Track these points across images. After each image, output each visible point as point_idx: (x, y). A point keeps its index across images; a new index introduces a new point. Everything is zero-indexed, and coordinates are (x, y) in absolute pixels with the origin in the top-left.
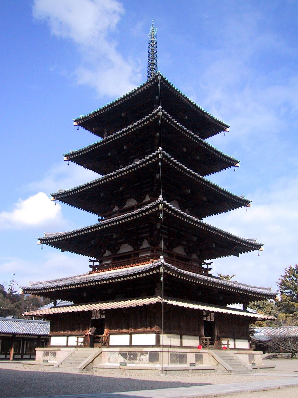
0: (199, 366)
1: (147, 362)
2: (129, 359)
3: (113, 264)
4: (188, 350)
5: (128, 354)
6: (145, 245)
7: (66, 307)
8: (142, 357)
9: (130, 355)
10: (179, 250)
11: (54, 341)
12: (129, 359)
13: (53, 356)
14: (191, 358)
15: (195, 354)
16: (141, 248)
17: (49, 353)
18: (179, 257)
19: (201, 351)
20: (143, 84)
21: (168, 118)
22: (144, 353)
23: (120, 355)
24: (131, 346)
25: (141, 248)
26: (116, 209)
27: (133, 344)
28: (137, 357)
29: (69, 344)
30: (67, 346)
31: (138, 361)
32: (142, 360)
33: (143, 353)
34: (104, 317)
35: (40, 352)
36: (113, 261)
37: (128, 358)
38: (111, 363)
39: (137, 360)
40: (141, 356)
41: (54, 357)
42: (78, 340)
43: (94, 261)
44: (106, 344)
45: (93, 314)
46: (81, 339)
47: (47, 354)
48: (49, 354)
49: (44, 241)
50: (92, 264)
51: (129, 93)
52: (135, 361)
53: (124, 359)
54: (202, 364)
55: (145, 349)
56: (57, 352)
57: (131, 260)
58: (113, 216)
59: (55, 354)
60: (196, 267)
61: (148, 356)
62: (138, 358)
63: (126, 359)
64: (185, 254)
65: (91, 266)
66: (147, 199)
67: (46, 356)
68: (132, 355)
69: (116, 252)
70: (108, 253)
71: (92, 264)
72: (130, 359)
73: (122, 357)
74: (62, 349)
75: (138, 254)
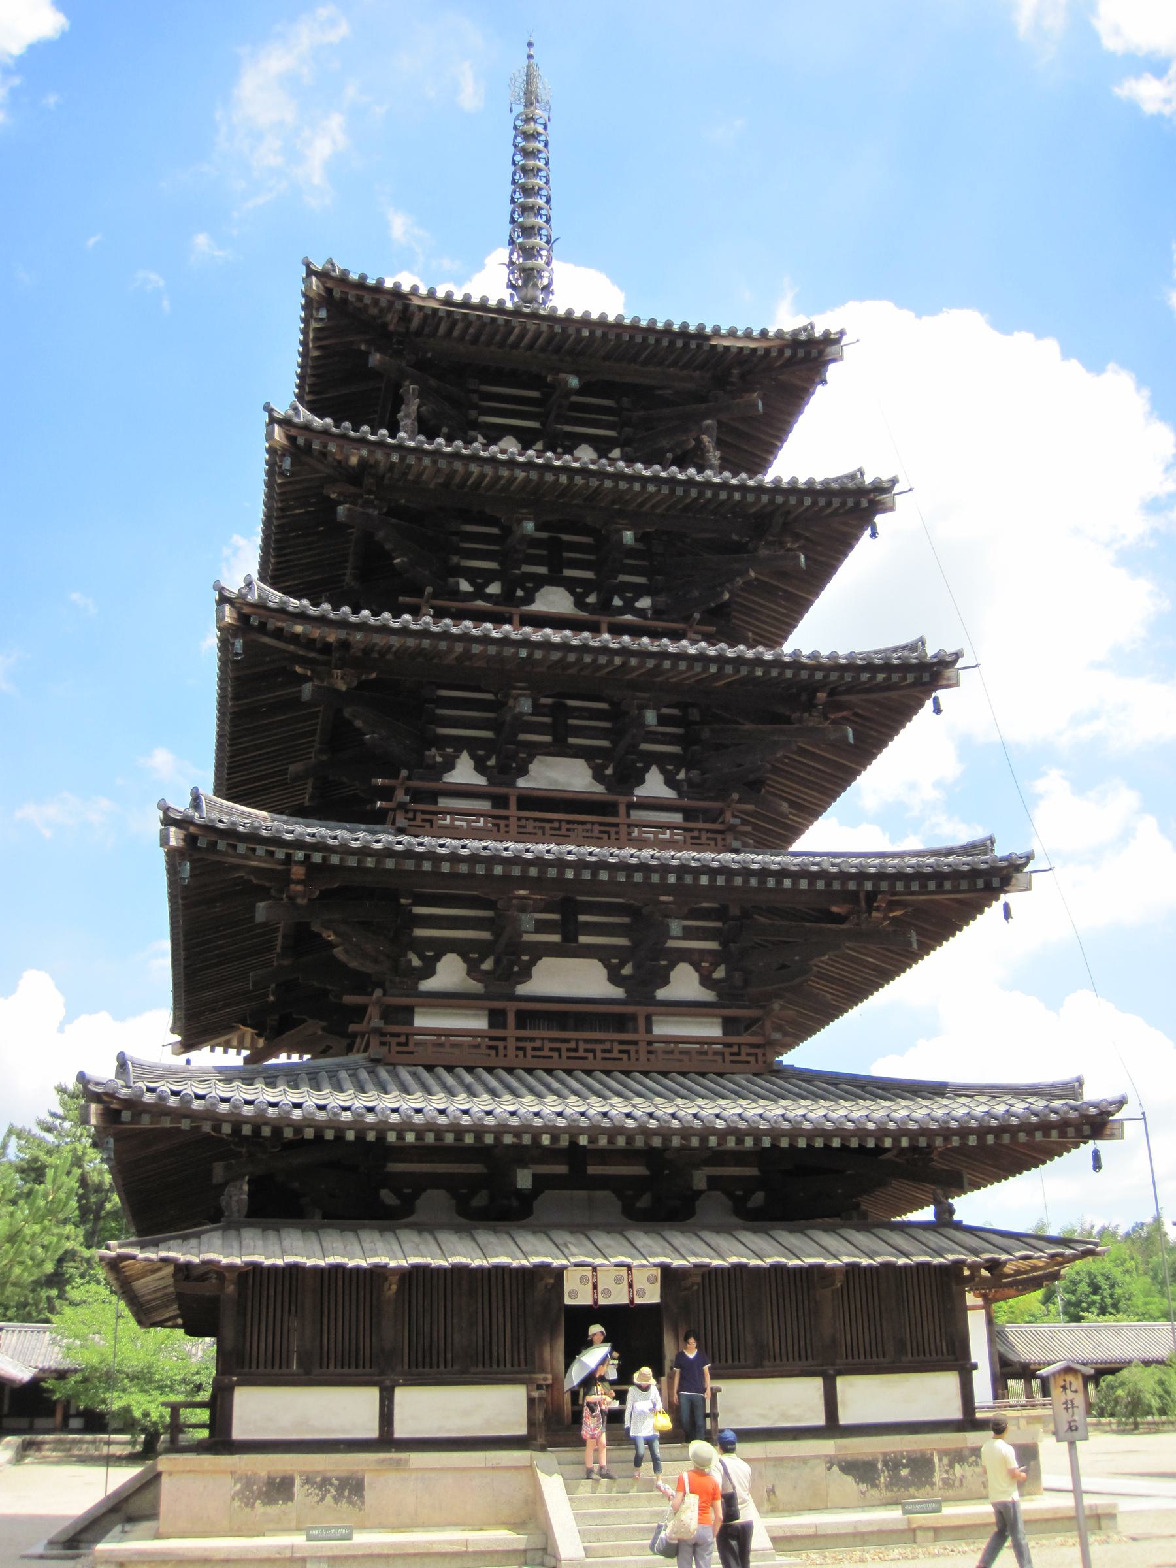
2: (887, 1487)
3: (492, 1038)
5: (880, 1465)
12: (888, 1487)
13: (336, 1499)
17: (298, 1482)
20: (764, 333)
22: (966, 1452)
23: (835, 1468)
26: (464, 773)
27: (845, 1418)
28: (932, 1471)
29: (401, 1431)
31: (938, 1491)
32: (957, 1483)
37: (882, 1480)
38: (781, 1511)
39: (933, 1484)
40: (951, 1465)
41: (344, 1505)
51: (685, 326)
52: (923, 1494)
53: (863, 1487)
57: (635, 1043)
58: (444, 803)
59: (352, 1488)
62: (938, 1477)
63: (874, 1484)
66: (654, 786)
68: (904, 1466)
72: (895, 1485)
73: (849, 1479)
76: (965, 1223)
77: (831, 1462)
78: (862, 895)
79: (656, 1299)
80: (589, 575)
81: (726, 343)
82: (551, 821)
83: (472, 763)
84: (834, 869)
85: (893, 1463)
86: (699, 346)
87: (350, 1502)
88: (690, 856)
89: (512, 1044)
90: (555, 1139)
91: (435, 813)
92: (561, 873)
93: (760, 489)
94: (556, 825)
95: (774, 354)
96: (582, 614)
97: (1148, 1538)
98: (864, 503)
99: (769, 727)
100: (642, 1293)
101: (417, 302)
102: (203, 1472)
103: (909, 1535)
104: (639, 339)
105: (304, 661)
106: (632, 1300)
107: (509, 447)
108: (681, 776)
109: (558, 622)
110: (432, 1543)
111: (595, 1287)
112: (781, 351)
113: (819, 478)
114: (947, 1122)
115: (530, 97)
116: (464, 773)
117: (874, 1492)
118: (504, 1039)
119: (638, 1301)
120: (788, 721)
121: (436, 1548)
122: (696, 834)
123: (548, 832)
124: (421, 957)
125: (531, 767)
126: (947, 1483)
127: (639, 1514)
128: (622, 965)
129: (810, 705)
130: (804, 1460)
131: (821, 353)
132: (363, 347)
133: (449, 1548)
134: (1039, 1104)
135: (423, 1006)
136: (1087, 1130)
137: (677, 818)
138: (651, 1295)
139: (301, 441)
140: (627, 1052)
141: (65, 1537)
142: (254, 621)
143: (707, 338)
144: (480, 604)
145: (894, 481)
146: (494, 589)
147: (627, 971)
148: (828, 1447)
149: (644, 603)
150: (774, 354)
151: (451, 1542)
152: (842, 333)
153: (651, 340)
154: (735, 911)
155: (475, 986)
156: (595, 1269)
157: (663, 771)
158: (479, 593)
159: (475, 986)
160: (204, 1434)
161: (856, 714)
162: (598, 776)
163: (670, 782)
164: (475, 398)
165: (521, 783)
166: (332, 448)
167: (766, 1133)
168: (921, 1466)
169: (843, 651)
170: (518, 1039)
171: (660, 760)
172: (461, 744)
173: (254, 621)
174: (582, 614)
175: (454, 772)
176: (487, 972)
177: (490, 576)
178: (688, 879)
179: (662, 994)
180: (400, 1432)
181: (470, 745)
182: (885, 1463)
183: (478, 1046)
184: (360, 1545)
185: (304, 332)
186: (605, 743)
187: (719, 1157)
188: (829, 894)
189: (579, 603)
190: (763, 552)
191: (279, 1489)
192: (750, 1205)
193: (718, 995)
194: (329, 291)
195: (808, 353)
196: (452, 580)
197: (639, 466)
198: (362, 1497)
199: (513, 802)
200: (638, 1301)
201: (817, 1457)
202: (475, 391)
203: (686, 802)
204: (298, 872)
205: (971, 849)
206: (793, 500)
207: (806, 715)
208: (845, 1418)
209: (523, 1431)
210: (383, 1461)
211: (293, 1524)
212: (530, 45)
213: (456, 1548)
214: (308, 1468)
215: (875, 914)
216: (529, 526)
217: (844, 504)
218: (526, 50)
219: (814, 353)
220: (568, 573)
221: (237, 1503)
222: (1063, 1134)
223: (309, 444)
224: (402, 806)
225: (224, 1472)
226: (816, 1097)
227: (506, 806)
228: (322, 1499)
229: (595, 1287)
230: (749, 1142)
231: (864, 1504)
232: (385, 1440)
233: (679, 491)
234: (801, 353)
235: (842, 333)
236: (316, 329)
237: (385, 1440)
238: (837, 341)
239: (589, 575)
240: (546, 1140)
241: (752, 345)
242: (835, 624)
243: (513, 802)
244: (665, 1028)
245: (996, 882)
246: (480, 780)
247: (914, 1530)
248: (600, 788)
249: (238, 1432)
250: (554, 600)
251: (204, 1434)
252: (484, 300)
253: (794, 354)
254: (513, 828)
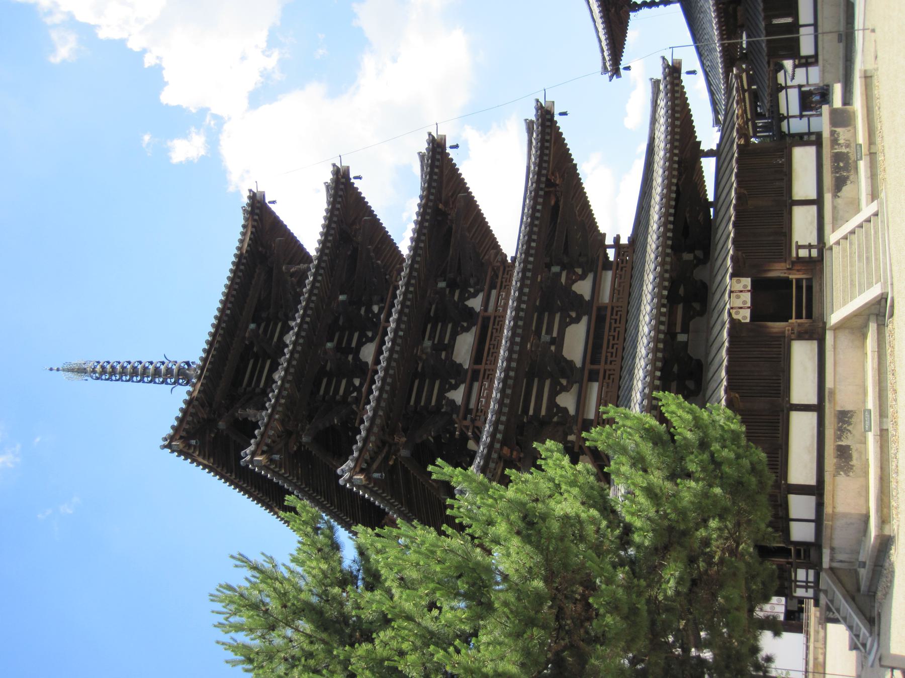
1: (852, 131)
8: (841, 141)
12: (848, 171)
13: (849, 424)
17: (840, 443)
23: (839, 194)
26: (457, 396)
27: (813, 195)
33: (835, 141)
39: (848, 153)
40: (839, 144)
41: (853, 420)
45: (739, 317)
51: (233, 263)
52: (852, 157)
53: (848, 182)
56: (838, 408)
58: (472, 405)
59: (844, 417)
61: (838, 130)
62: (844, 150)
66: (476, 303)
67: (850, 457)
73: (845, 189)
76: (718, 142)
77: (835, 196)
78: (547, 190)
79: (749, 279)
80: (356, 335)
81: (246, 245)
82: (489, 349)
83: (452, 392)
84: (534, 185)
85: (836, 169)
86: (245, 258)
87: (851, 417)
88: (514, 293)
89: (608, 367)
90: (664, 306)
91: (477, 410)
92: (522, 310)
93: (319, 258)
94: (492, 347)
95: (256, 224)
96: (377, 339)
97: (876, 51)
98: (343, 180)
99: (453, 240)
100: (745, 286)
101: (195, 394)
102: (834, 491)
103: (872, 155)
104: (237, 287)
105: (386, 459)
106: (749, 291)
107: (290, 338)
108: (472, 290)
109: (379, 352)
110: (873, 368)
111: (741, 308)
112: (255, 220)
113: (325, 206)
114: (649, 349)
115: (81, 371)
116: (457, 396)
117: (851, 178)
118: (605, 371)
119: (749, 288)
120: (451, 228)
121: (876, 365)
122: (492, 347)
123: (495, 350)
124: (556, 414)
125: (458, 362)
126: (848, 146)
127: (859, 268)
128: (570, 317)
129: (444, 214)
130: (834, 208)
131: (259, 202)
132: (213, 435)
133: (876, 360)
134: (662, 95)
135: (583, 414)
136: (675, 75)
137: (494, 293)
138: (747, 282)
139: (265, 448)
140: (609, 375)
141: (869, 626)
142: (364, 466)
143: (241, 254)
144: (364, 389)
145: (334, 165)
146: (357, 382)
147: (574, 314)
148: (828, 197)
149: (376, 309)
150: (256, 224)
151: (873, 359)
152: (250, 191)
153: (238, 280)
154: (548, 260)
155: (575, 388)
156: (732, 308)
157: (468, 299)
158: (358, 389)
159: (575, 388)
160: (811, 573)
161: (453, 195)
162: (467, 330)
163: (475, 295)
164: (249, 389)
165: (466, 366)
166: (271, 433)
167: (655, 355)
168: (838, 157)
169: (419, 192)
170: (606, 363)
171: (463, 299)
172: (441, 396)
173: (364, 466)
174: (377, 339)
175: (456, 400)
176: (568, 382)
177: (350, 383)
178: (532, 252)
179: (587, 297)
180: (812, 481)
181: (442, 392)
182: (837, 173)
183: (608, 384)
184: (874, 406)
185: (199, 464)
186: (450, 326)
187: (671, 324)
188: (544, 204)
189: (371, 340)
190: (360, 239)
191: (844, 453)
192: (702, 257)
193: (591, 271)
194: (181, 438)
195: (258, 208)
196: (349, 399)
197: (307, 281)
198: (848, 412)
199: (477, 367)
200: (749, 304)
201: (833, 202)
202: (245, 389)
203: (486, 287)
204: (506, 451)
205: (530, 131)
206: (337, 213)
207: (449, 217)
208: (813, 195)
209: (814, 344)
210: (829, 400)
211: (863, 446)
212: (51, 369)
213: (876, 356)
214: (832, 437)
215: (557, 182)
216: (329, 345)
217: (342, 190)
218: (54, 372)
219: (258, 205)
220: (354, 345)
221: (851, 474)
222: (677, 92)
223: (267, 445)
224: (473, 421)
225: (834, 481)
226: (649, 206)
227: (479, 371)
228: (850, 431)
229: (741, 308)
230: (663, 319)
231: (857, 182)
232: (819, 408)
233: (323, 265)
234: (257, 211)
235: (250, 191)
236: (199, 455)
237: (819, 408)
238: (254, 194)
239: (356, 335)
240: (664, 310)
241: (249, 233)
242: (399, 216)
243: (477, 367)
244: (606, 296)
245: (548, 117)
246: (462, 388)
247: (871, 154)
248: (474, 329)
249: (812, 481)
250: (368, 353)
251: (811, 573)
252: (204, 350)
253: (257, 214)
254: (492, 367)
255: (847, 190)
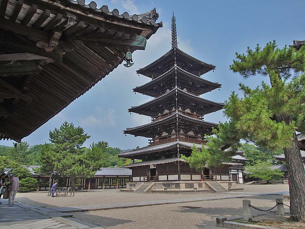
0: (201, 189)
4: (195, 182)
6: (174, 132)
7: (139, 162)
9: (167, 185)
10: (191, 133)
11: (135, 179)
14: (196, 186)
15: (198, 183)
16: (172, 133)
18: (190, 137)
19: (201, 182)
21: (180, 70)
24: (168, 180)
25: (172, 133)
26: (160, 114)
30: (140, 181)
33: (173, 184)
34: (155, 167)
35: (128, 185)
36: (160, 140)
42: (144, 178)
43: (151, 140)
44: (157, 180)
46: (146, 178)
47: (131, 185)
48: (132, 185)
49: (126, 132)
50: (150, 142)
54: (202, 188)
55: (173, 182)
59: (134, 185)
60: (200, 140)
64: (194, 135)
65: (149, 143)
66: (174, 109)
69: (161, 136)
70: (157, 136)
71: (150, 142)
74: (138, 183)
75: (171, 136)
212: (173, 13)
255: (163, 187)
